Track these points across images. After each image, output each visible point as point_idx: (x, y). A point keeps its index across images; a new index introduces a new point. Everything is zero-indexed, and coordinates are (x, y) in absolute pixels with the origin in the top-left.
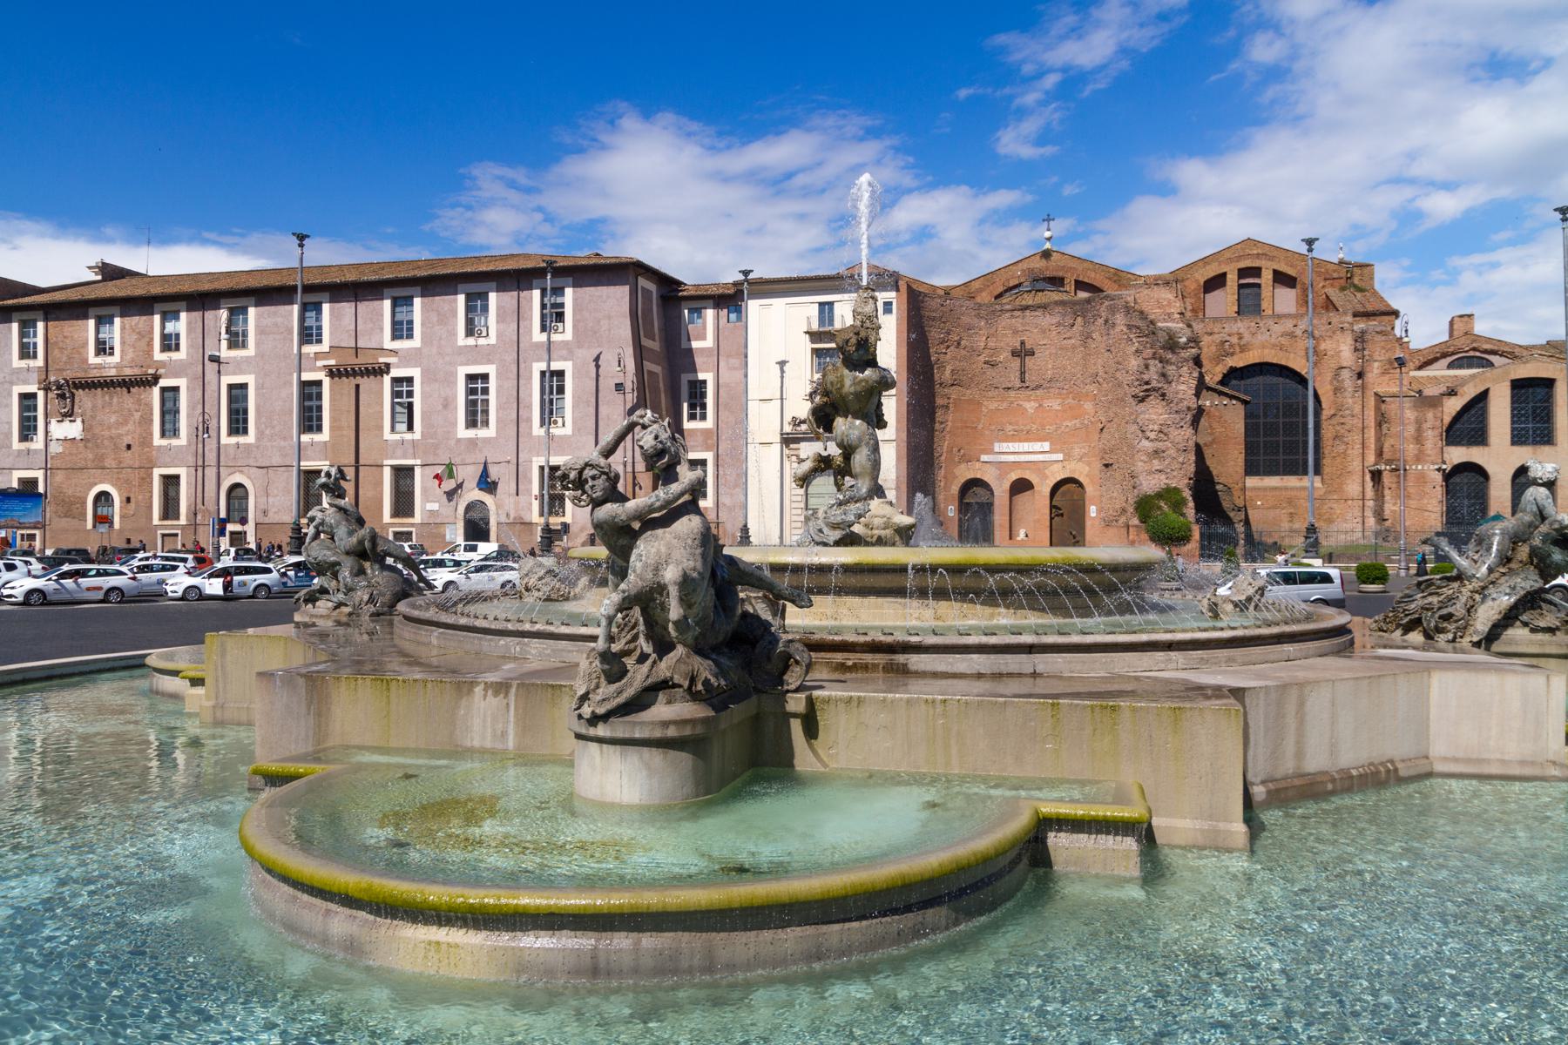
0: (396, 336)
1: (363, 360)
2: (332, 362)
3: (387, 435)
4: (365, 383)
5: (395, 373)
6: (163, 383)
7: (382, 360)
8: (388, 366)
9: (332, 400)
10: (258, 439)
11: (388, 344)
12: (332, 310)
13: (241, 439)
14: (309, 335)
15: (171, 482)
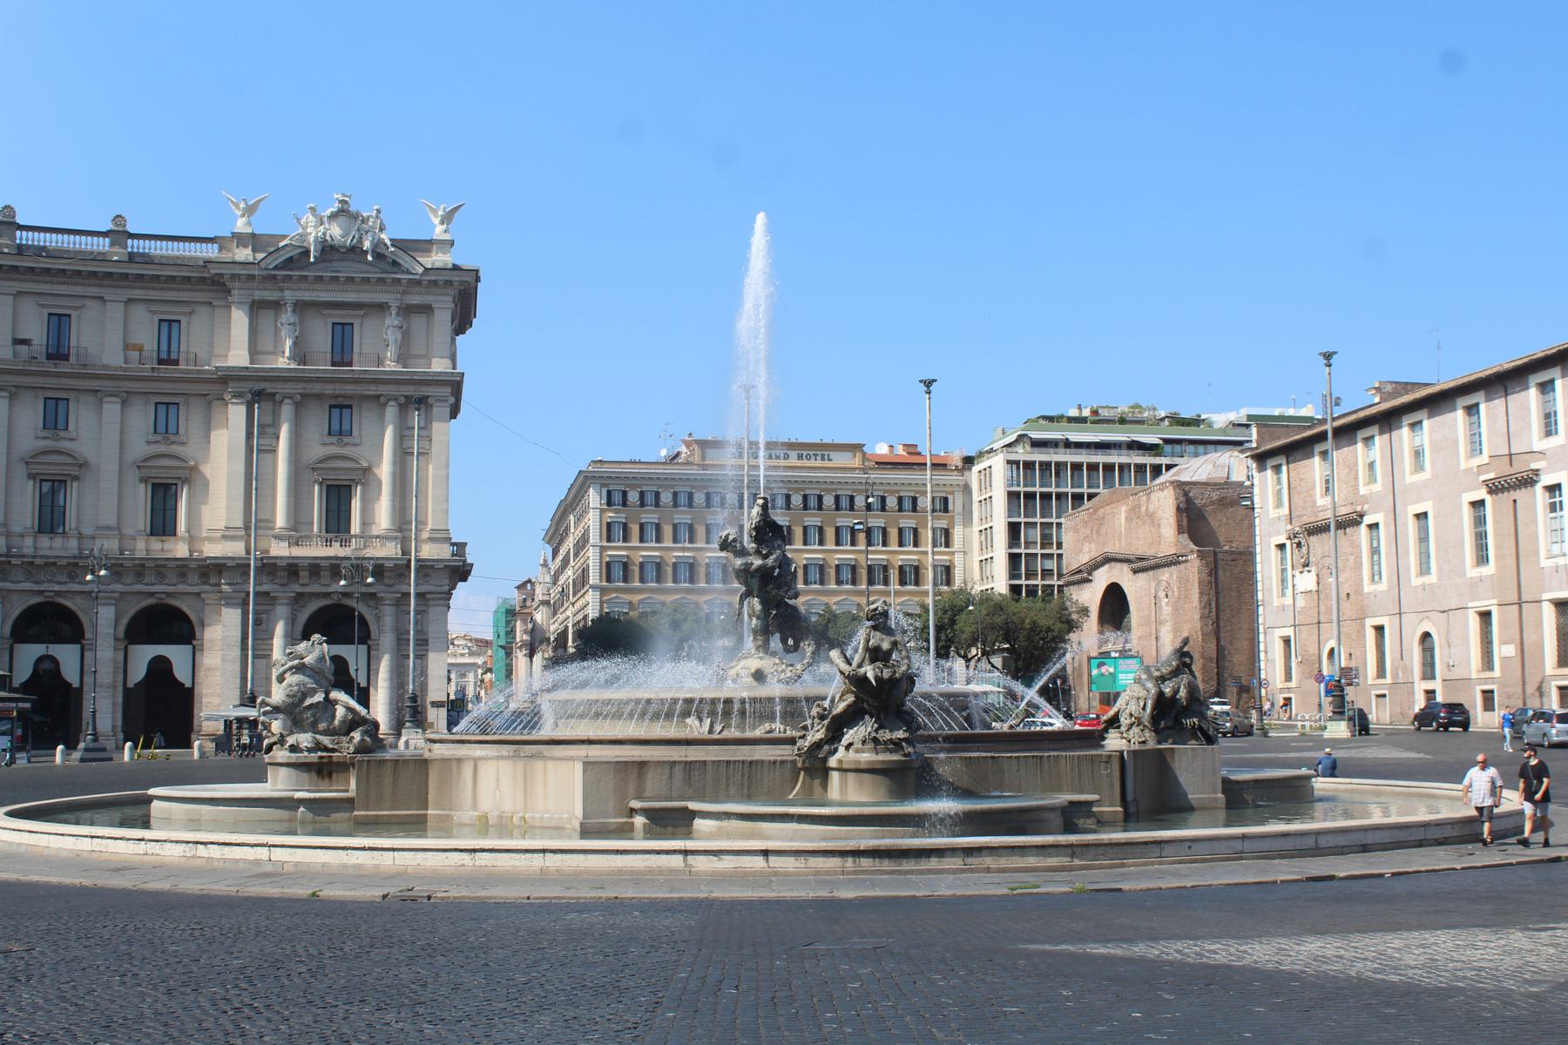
0: (1548, 433)
1: (1520, 467)
2: (1492, 475)
3: (1545, 563)
4: (1521, 495)
5: (1546, 479)
6: (1368, 520)
7: (1534, 466)
8: (1536, 472)
9: (1495, 522)
10: (1439, 577)
11: (1539, 444)
12: (1487, 409)
13: (1426, 580)
14: (1475, 447)
15: (1380, 629)
